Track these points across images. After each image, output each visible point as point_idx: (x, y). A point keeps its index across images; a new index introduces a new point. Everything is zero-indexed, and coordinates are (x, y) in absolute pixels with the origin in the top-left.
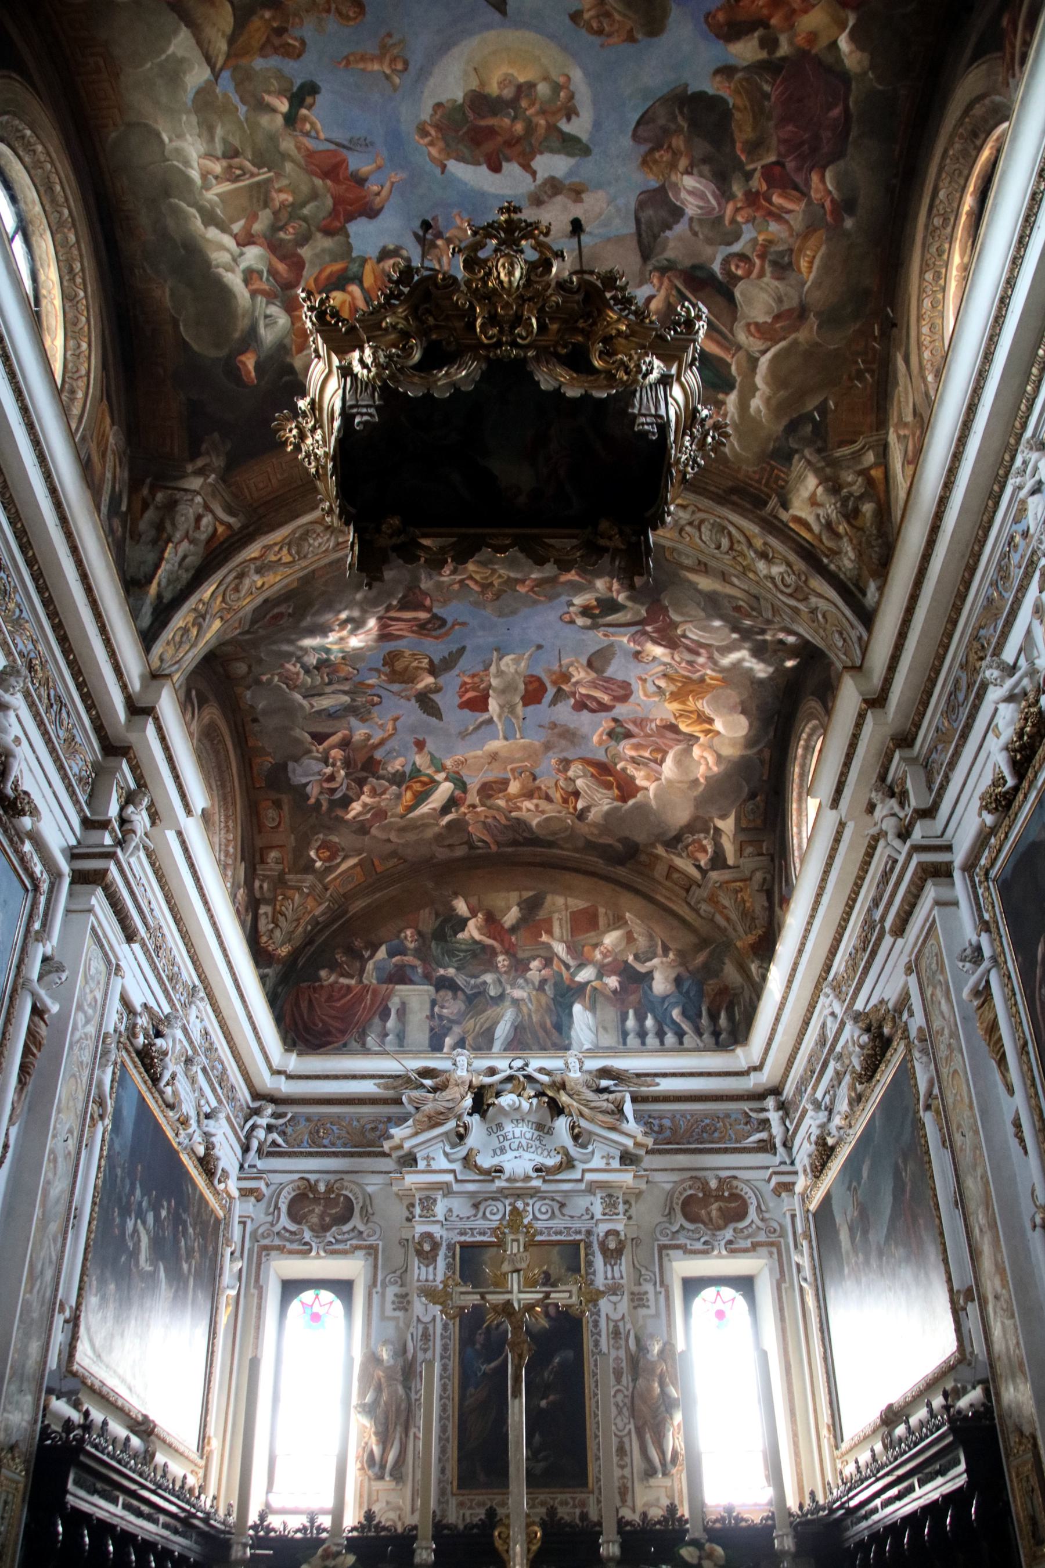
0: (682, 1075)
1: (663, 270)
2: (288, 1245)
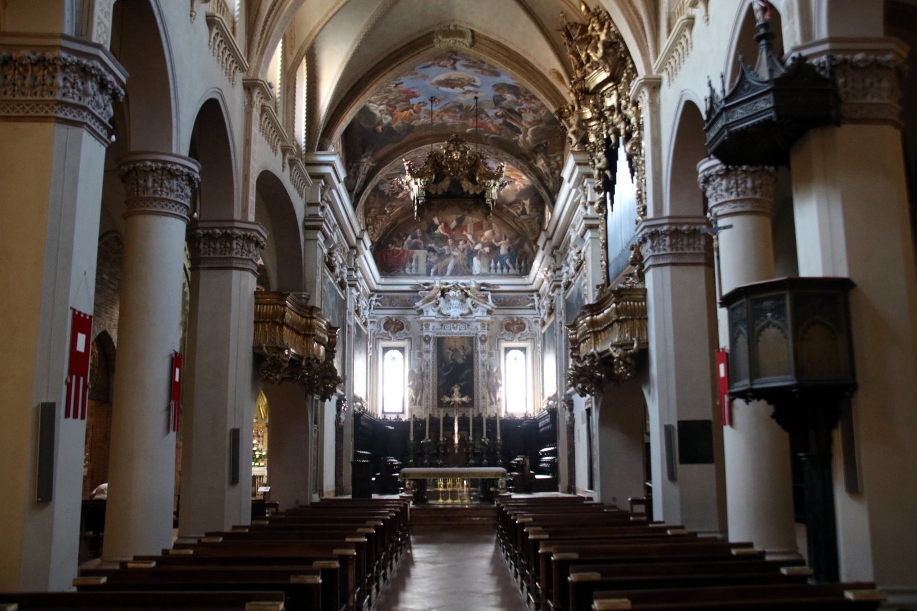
0: (508, 285)
1: (502, 108)
2: (385, 338)
